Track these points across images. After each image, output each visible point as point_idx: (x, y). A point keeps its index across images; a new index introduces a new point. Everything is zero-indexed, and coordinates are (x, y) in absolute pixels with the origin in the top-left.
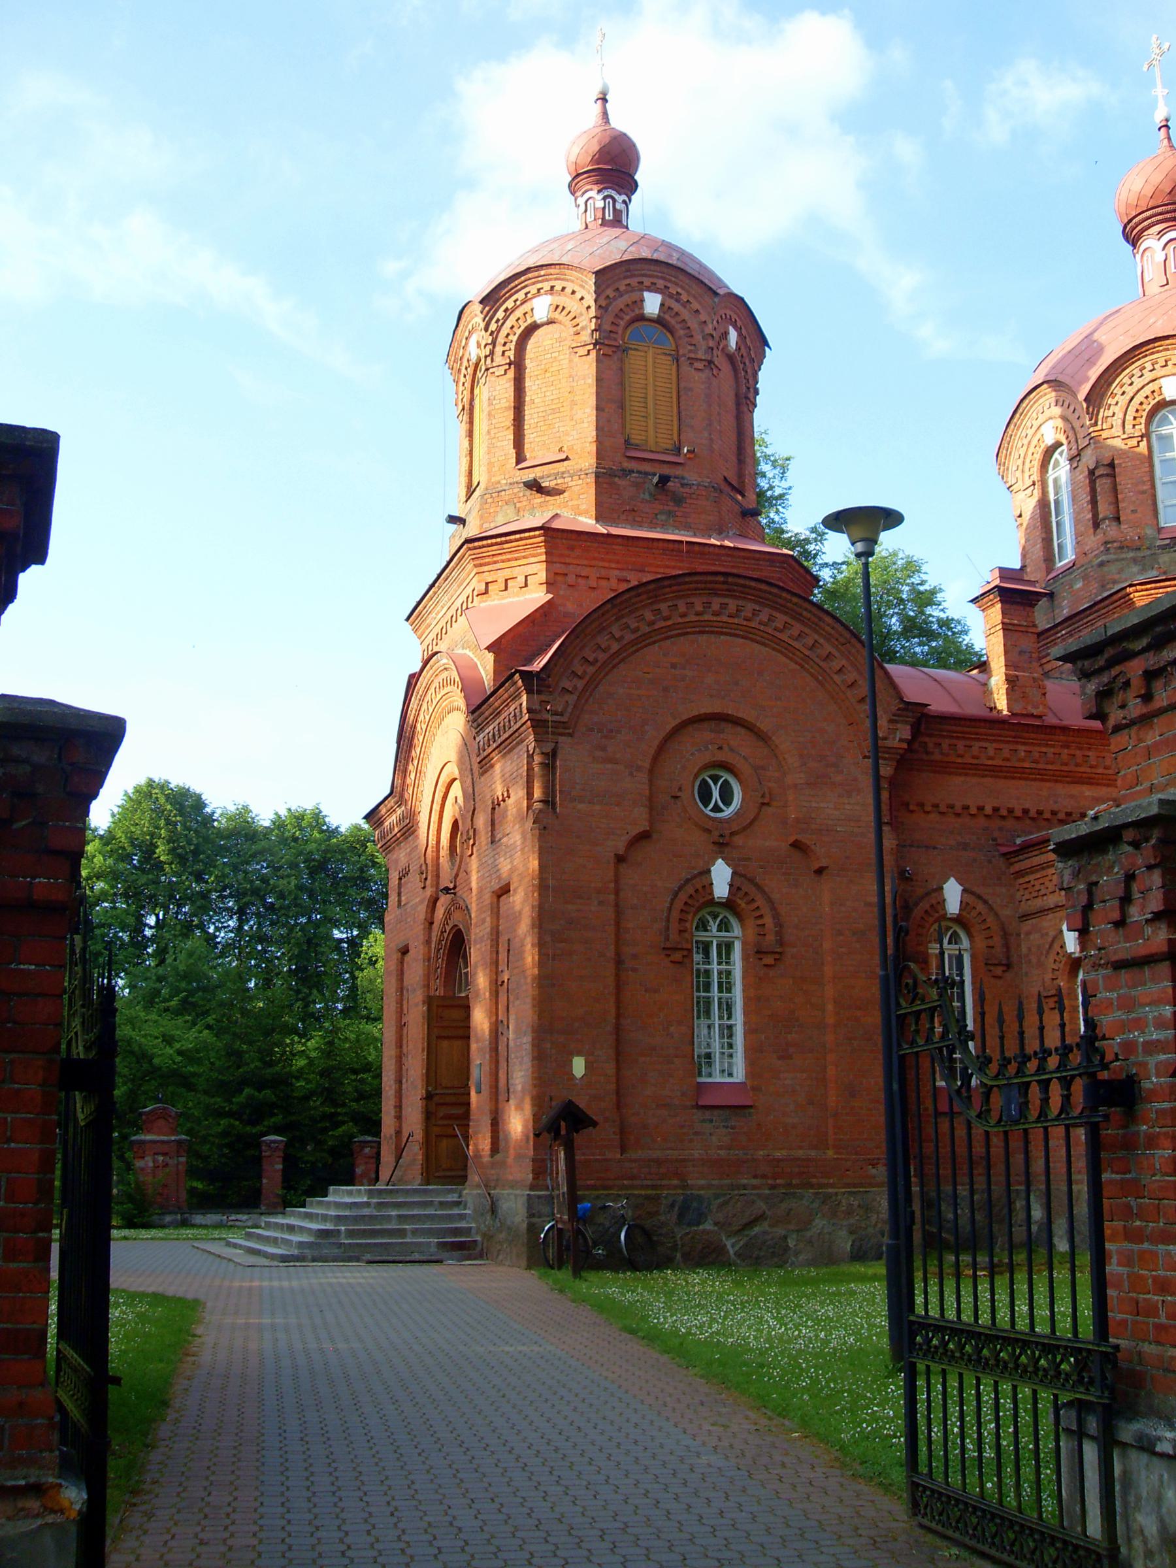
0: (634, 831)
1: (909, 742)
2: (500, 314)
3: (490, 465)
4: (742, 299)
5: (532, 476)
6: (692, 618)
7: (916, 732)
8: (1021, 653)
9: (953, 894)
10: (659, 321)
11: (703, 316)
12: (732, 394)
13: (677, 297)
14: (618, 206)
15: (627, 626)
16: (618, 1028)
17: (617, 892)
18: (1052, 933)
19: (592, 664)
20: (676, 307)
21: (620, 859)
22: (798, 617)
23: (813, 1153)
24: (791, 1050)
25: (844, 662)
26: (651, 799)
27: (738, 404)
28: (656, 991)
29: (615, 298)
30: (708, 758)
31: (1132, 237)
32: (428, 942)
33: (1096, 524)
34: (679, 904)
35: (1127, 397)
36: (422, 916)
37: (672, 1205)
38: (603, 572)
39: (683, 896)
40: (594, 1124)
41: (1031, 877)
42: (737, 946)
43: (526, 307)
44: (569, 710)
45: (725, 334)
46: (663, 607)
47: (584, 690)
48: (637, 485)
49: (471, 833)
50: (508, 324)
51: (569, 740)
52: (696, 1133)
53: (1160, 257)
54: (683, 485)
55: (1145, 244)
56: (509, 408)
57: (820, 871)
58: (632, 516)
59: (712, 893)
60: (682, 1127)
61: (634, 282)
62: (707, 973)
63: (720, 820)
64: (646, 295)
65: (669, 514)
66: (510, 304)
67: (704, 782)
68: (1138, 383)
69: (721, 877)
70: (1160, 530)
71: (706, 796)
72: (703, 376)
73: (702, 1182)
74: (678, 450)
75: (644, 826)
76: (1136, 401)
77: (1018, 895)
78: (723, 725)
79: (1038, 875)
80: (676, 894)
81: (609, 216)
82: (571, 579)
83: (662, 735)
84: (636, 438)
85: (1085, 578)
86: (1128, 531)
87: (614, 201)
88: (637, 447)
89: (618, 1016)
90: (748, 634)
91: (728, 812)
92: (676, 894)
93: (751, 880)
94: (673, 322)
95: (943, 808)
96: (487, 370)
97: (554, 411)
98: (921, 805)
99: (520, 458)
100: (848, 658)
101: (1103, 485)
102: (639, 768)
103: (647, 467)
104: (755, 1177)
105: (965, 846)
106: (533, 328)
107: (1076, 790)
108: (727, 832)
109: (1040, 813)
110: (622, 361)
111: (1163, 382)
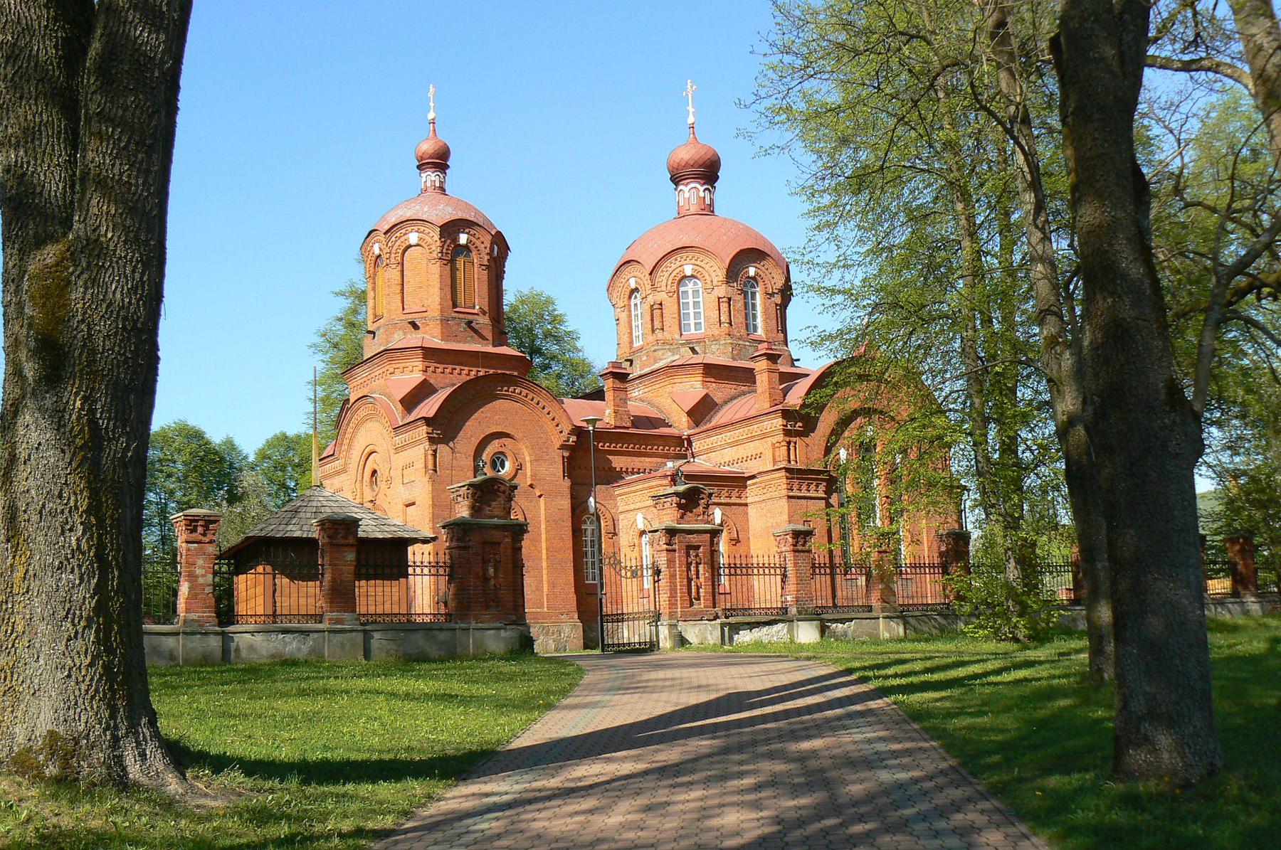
20: (474, 240)
22: (532, 391)
31: (676, 179)
33: (653, 331)
53: (687, 195)
55: (681, 187)
58: (455, 338)
68: (674, 266)
101: (657, 313)
106: (410, 246)
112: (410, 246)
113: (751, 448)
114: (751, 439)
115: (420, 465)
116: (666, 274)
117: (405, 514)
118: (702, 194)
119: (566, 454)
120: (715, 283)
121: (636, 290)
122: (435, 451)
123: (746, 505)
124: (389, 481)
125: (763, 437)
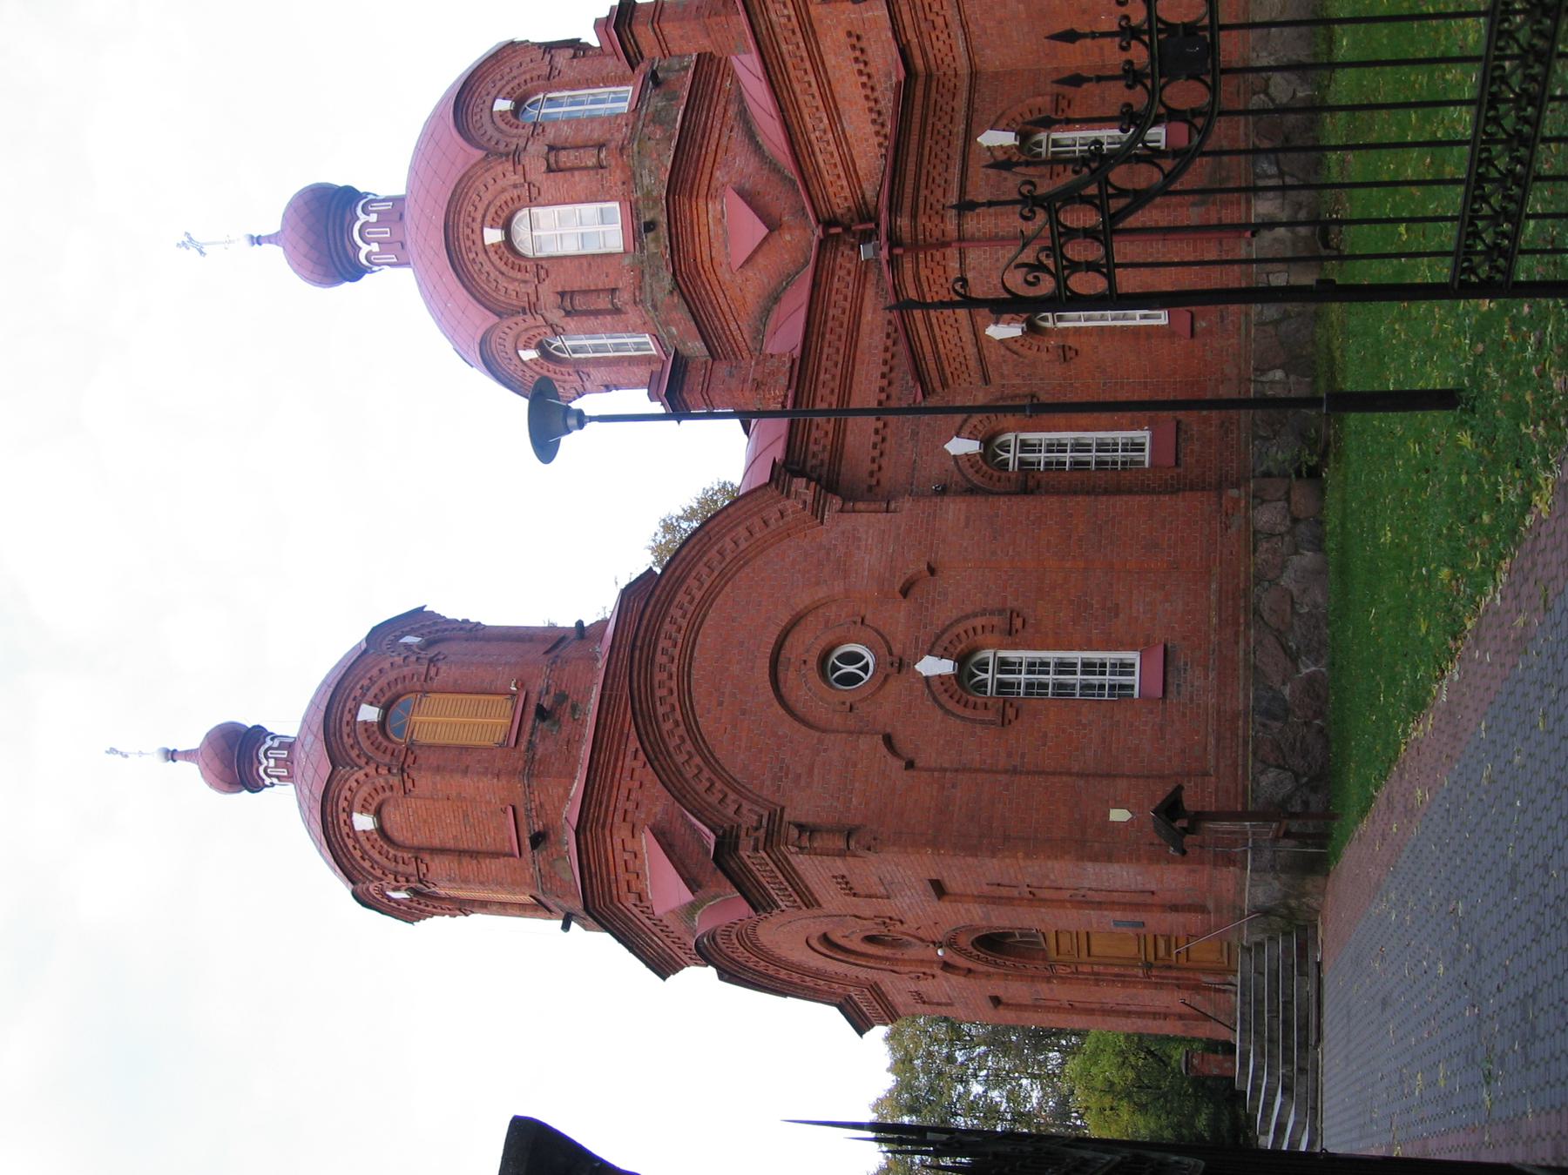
0: (884, 751)
1: (810, 479)
2: (367, 864)
3: (514, 883)
4: (375, 631)
5: (527, 842)
6: (674, 684)
7: (801, 474)
8: (731, 375)
9: (961, 446)
10: (386, 709)
11: (387, 665)
12: (465, 644)
13: (365, 690)
14: (276, 744)
15: (678, 747)
16: (1080, 775)
17: (945, 770)
18: (1003, 351)
19: (712, 784)
21: (910, 765)
23: (1214, 586)
24: (1109, 604)
25: (727, 539)
26: (851, 733)
27: (476, 639)
28: (1045, 735)
29: (361, 749)
30: (814, 676)
32: (988, 975)
33: (617, 311)
34: (958, 709)
35: (500, 279)
36: (962, 979)
37: (1264, 725)
38: (626, 774)
39: (951, 705)
40: (1180, 788)
41: (948, 371)
42: (1002, 654)
43: (362, 839)
44: (757, 808)
45: (407, 646)
46: (661, 710)
47: (738, 792)
48: (543, 739)
49: (879, 920)
50: (377, 857)
51: (787, 810)
52: (1191, 700)
53: (375, 247)
54: (547, 693)
56: (460, 863)
57: (932, 571)
58: (572, 743)
59: (949, 677)
60: (1184, 715)
61: (346, 729)
62: (1030, 685)
63: (877, 665)
64: (360, 718)
65: (574, 708)
66: (357, 854)
67: (838, 680)
68: (487, 267)
69: (934, 666)
70: (625, 252)
71: (851, 679)
72: (443, 668)
73: (1241, 695)
74: (513, 694)
75: (879, 739)
76: (504, 269)
77: (965, 385)
78: (782, 659)
79: (946, 364)
80: (948, 712)
81: (284, 754)
82: (630, 806)
83: (787, 717)
84: (499, 737)
85: (666, 324)
86: (625, 281)
87: (270, 748)
88: (507, 737)
89: (1070, 774)
90: (695, 628)
91: (869, 658)
92: (948, 712)
93: (938, 637)
94: (388, 694)
95: (876, 453)
96: (420, 881)
97: (466, 815)
98: (872, 474)
99: (512, 855)
100: (724, 535)
102: (820, 741)
103: (527, 727)
104: (1237, 643)
105: (915, 434)
107: (865, 329)
108: (889, 659)
109: (885, 362)
110: (421, 746)
111: (488, 242)
112: (381, 830)
113: (840, 64)
114: (817, 62)
115: (840, 866)
116: (503, 283)
117: (960, 897)
118: (373, 218)
119: (836, 502)
120: (518, 179)
121: (541, 346)
122: (801, 827)
123: (974, 75)
124: (888, 921)
125: (808, 29)
